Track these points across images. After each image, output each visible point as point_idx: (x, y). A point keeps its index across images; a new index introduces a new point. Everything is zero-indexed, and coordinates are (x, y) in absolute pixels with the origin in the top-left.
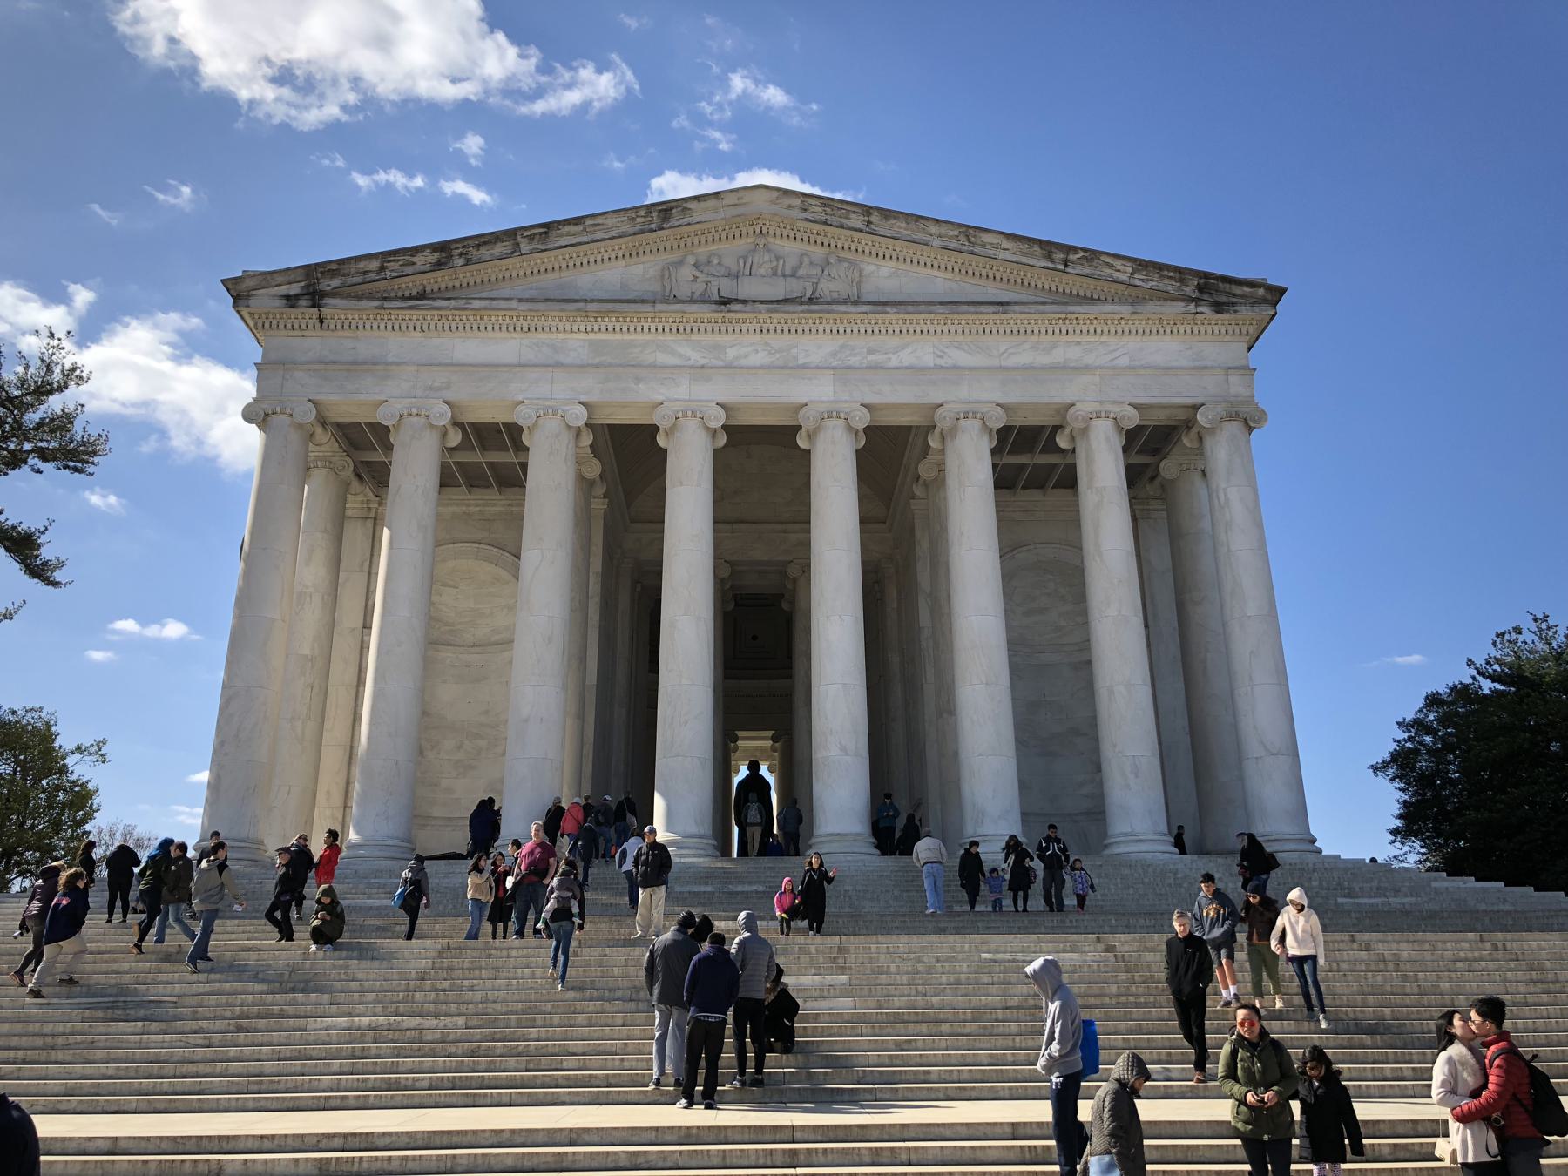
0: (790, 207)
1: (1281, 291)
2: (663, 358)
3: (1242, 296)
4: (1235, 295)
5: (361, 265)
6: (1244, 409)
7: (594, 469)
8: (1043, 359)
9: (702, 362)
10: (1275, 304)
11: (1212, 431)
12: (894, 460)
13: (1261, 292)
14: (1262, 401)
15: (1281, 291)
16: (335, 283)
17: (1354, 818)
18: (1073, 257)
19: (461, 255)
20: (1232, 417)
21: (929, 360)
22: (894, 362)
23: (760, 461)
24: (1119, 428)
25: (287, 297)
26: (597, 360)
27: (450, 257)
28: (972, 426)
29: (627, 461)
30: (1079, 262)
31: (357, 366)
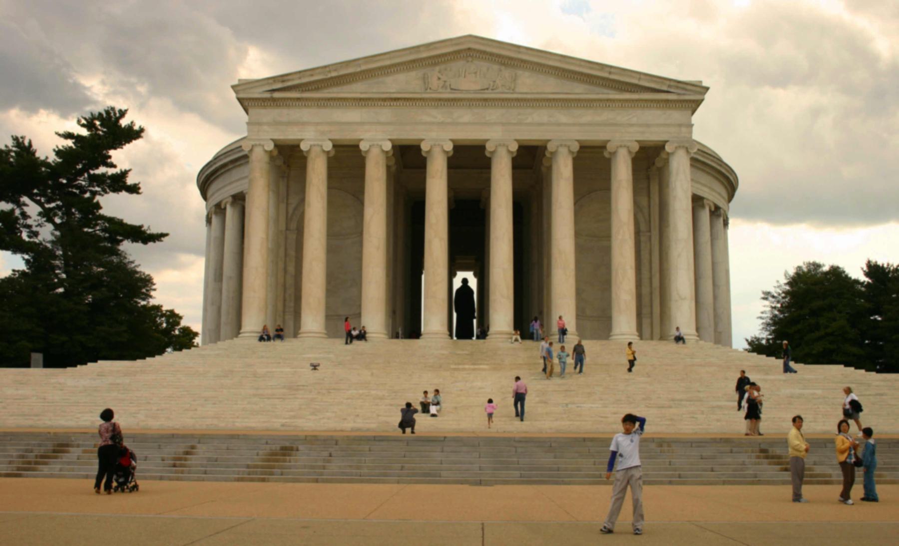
1: (707, 89)
3: (691, 90)
4: (686, 90)
6: (687, 145)
7: (392, 162)
8: (598, 119)
10: (705, 93)
11: (673, 153)
12: (531, 161)
13: (698, 89)
15: (707, 89)
17: (749, 318)
18: (612, 70)
21: (545, 119)
22: (529, 120)
23: (469, 161)
24: (630, 152)
27: (330, 72)
28: (563, 151)
29: (408, 160)
30: (614, 73)
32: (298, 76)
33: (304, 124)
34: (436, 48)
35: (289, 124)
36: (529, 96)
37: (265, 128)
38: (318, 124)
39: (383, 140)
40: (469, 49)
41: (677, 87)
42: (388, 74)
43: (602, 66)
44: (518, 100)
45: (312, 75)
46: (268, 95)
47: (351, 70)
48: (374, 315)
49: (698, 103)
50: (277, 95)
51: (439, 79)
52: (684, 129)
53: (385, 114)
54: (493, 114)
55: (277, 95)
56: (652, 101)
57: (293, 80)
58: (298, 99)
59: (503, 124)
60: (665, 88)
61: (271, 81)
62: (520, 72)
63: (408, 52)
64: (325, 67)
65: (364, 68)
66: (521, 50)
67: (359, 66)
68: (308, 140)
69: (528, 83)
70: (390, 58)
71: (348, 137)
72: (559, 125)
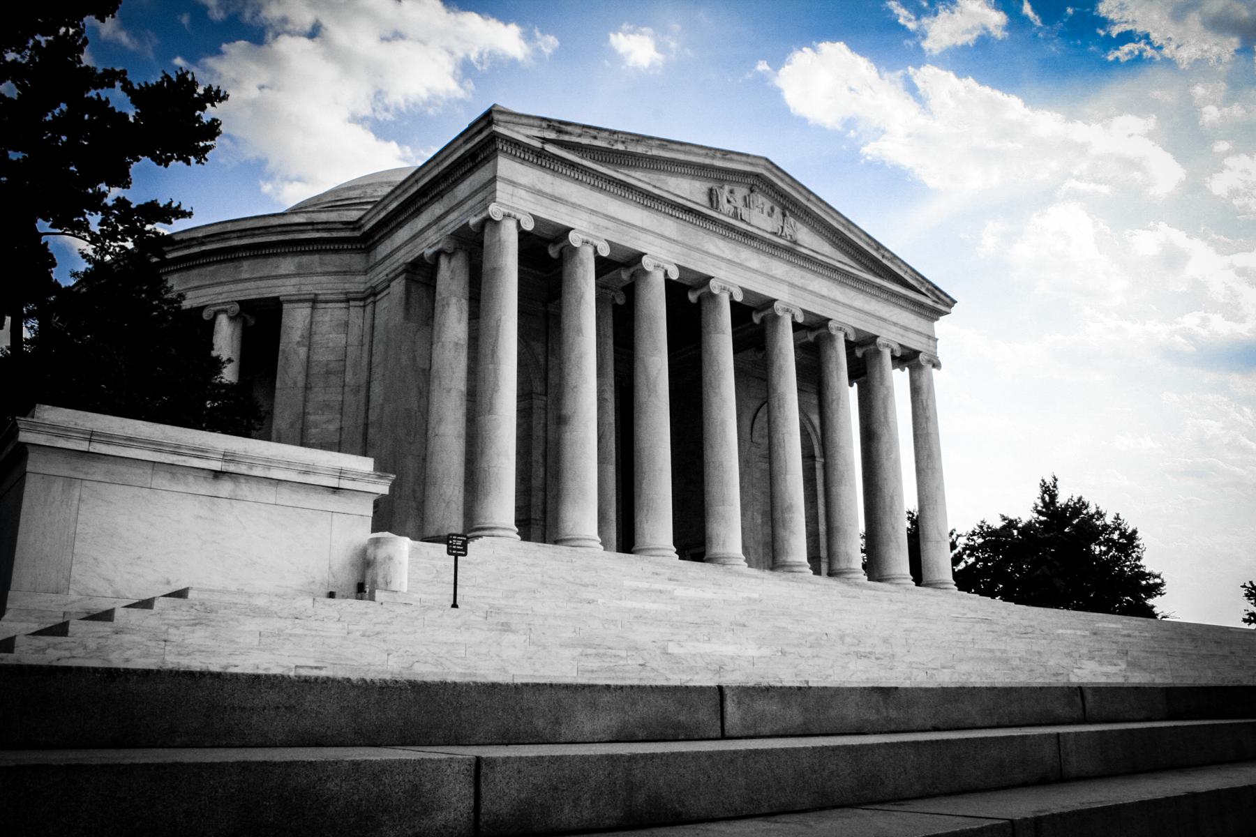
0: (776, 175)
1: (955, 302)
2: (712, 249)
5: (569, 129)
9: (729, 257)
10: (950, 306)
14: (941, 355)
15: (955, 302)
16: (553, 136)
19: (623, 142)
20: (929, 361)
21: (824, 292)
25: (528, 136)
26: (680, 239)
27: (616, 141)
31: (555, 199)
32: (578, 131)
33: (574, 205)
34: (731, 160)
35: (555, 199)
36: (819, 257)
37: (522, 193)
38: (593, 212)
39: (669, 263)
40: (758, 176)
41: (933, 293)
42: (672, 173)
43: (879, 247)
44: (807, 258)
45: (595, 138)
46: (537, 144)
47: (640, 149)
48: (659, 524)
49: (942, 313)
50: (550, 148)
51: (729, 201)
52: (931, 342)
53: (669, 226)
54: (779, 268)
55: (550, 148)
56: (906, 298)
57: (567, 133)
58: (573, 165)
59: (792, 285)
60: (923, 290)
61: (544, 124)
62: (799, 225)
63: (704, 152)
64: (614, 132)
65: (655, 152)
66: (812, 198)
67: (651, 147)
68: (581, 232)
69: (808, 239)
70: (685, 152)
71: (628, 245)
72: (837, 302)
